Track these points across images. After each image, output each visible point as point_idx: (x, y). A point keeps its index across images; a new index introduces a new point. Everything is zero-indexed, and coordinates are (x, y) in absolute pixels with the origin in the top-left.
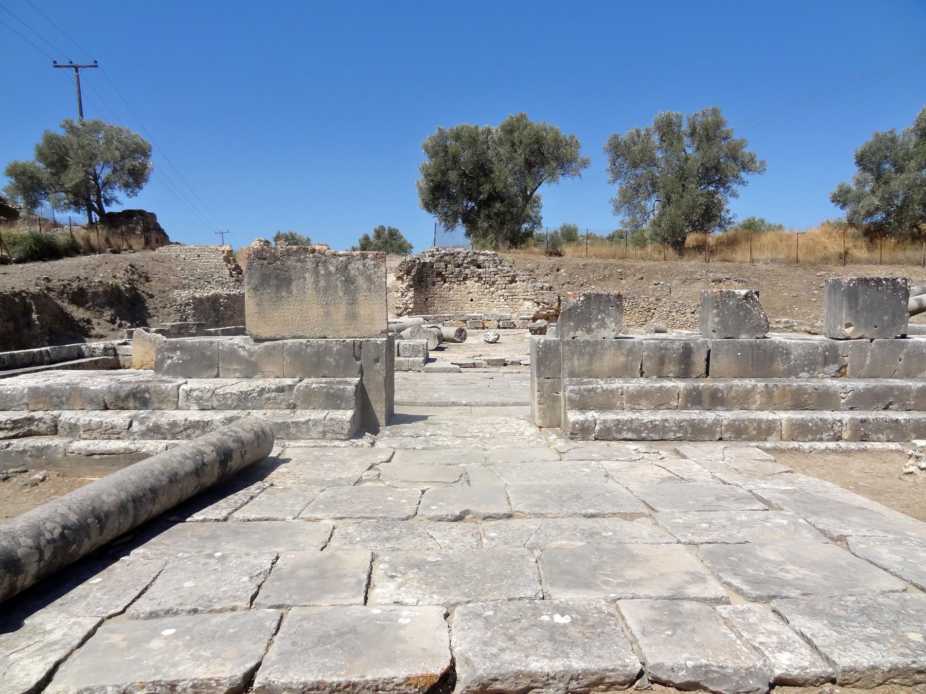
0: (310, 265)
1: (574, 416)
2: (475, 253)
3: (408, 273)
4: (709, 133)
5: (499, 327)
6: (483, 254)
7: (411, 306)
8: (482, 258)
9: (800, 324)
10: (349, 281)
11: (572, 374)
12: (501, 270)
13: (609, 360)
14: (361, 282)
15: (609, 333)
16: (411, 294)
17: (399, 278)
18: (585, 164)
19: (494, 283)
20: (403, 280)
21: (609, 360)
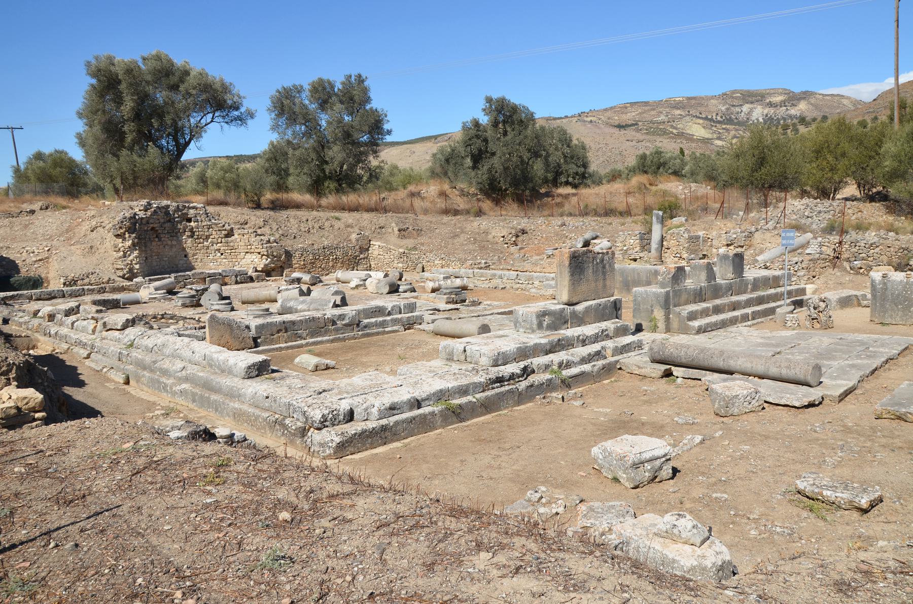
0: (591, 260)
1: (696, 324)
2: (185, 207)
3: (131, 230)
4: (354, 96)
5: (237, 283)
6: (193, 208)
7: (137, 266)
8: (192, 211)
9: (493, 264)
10: (604, 267)
11: (675, 306)
12: (216, 224)
13: (684, 297)
14: (607, 266)
15: (682, 285)
16: (136, 253)
17: (117, 236)
18: (251, 115)
19: (207, 237)
20: (124, 239)
21: (684, 297)
